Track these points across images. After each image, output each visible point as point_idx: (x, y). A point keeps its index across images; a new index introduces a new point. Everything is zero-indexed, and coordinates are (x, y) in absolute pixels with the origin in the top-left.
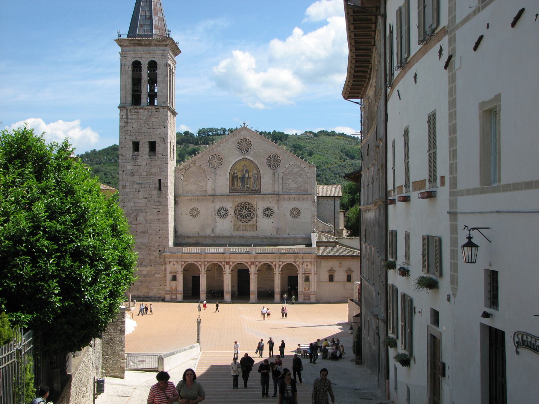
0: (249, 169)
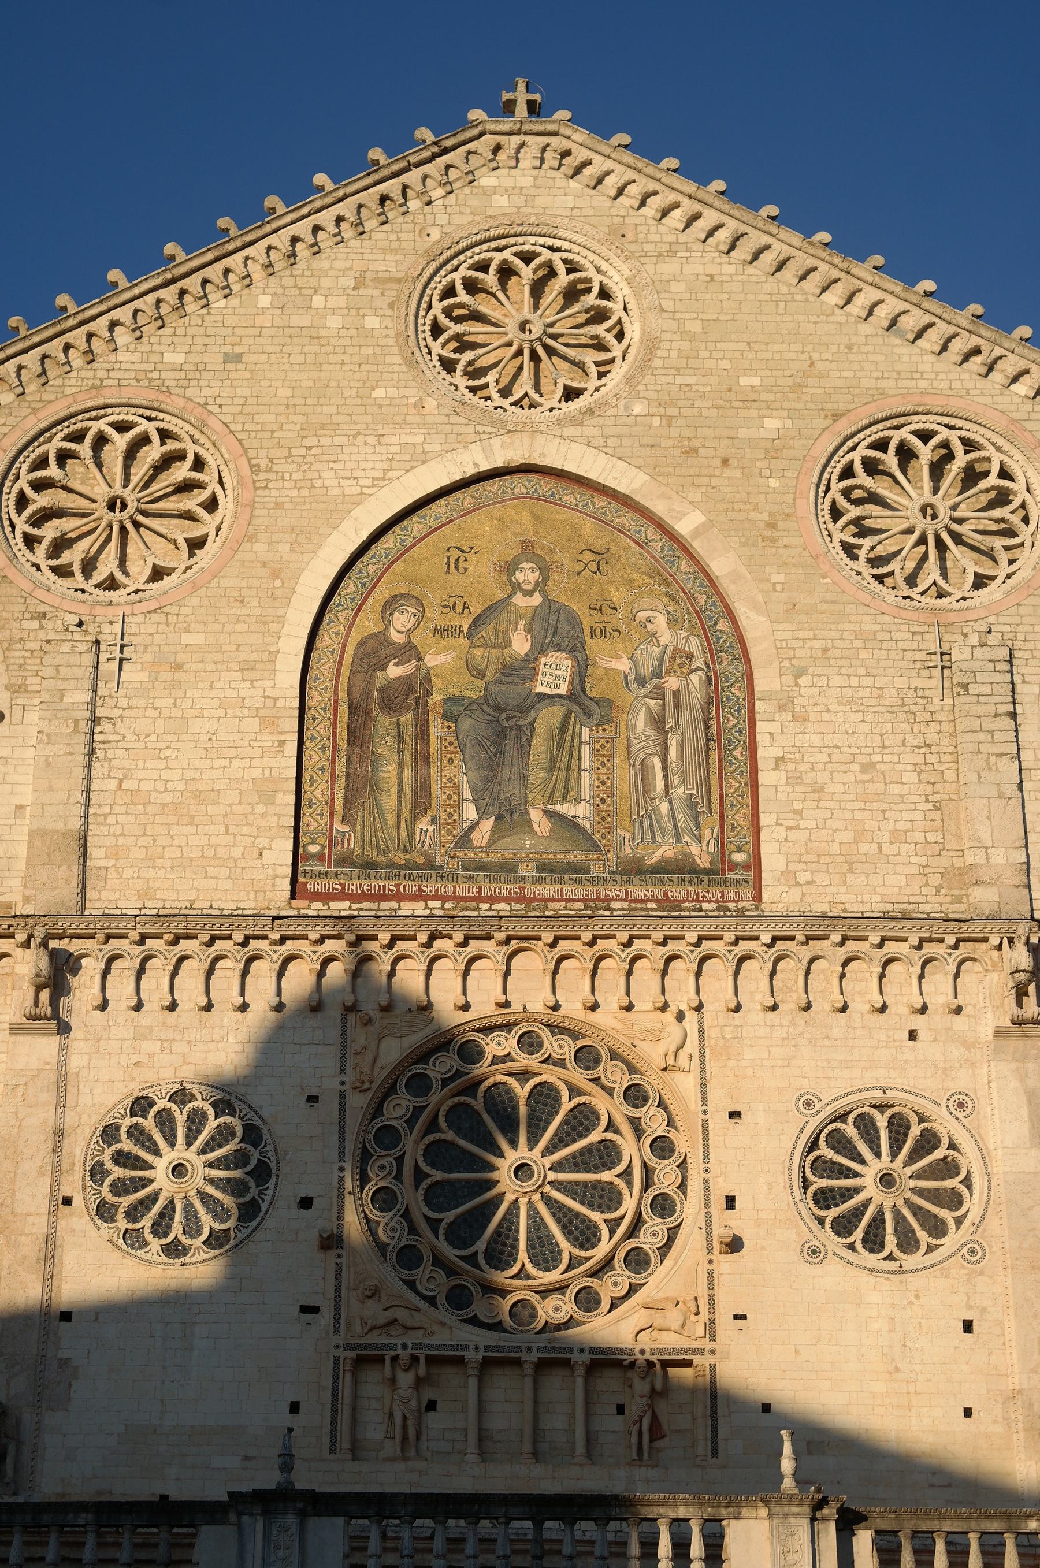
0: (578, 607)
